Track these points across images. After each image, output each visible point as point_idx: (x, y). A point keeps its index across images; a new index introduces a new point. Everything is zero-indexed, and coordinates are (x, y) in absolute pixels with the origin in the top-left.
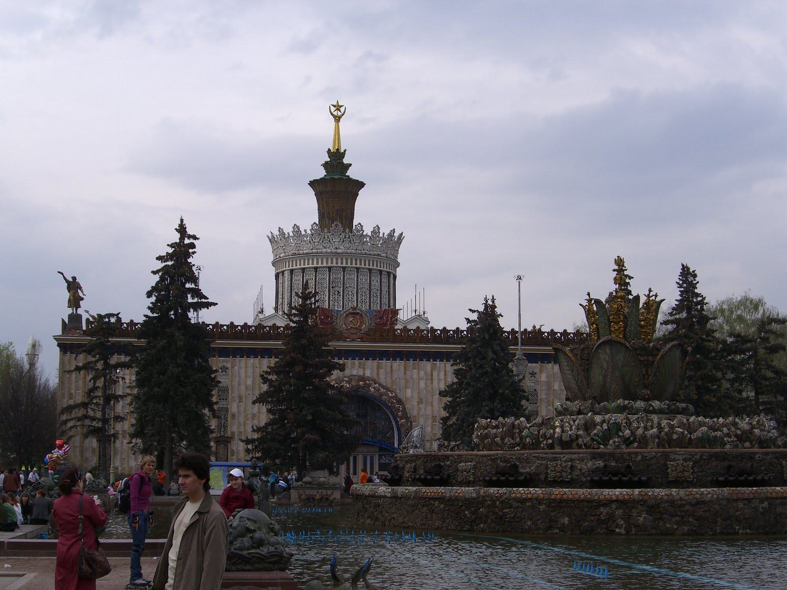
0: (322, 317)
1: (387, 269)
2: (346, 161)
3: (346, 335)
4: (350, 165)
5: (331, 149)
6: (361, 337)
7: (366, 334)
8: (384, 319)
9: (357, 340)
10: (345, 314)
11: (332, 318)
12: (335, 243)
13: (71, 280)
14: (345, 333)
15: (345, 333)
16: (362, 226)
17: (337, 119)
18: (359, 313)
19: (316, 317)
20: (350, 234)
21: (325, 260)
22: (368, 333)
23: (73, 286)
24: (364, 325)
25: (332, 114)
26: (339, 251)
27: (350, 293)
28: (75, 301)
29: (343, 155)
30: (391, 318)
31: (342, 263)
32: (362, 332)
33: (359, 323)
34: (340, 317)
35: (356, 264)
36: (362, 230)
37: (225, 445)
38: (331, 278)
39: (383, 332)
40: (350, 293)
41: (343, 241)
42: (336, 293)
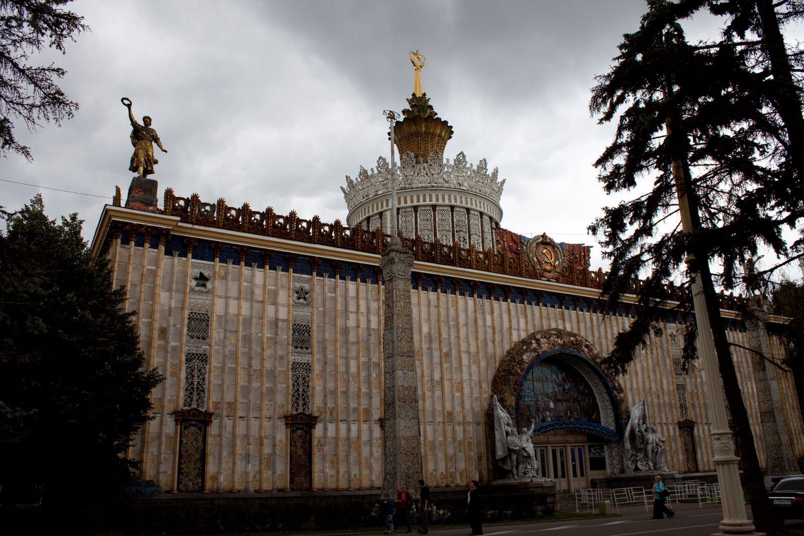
12: (459, 178)
13: (141, 123)
17: (418, 68)
26: (462, 188)
42: (462, 239)
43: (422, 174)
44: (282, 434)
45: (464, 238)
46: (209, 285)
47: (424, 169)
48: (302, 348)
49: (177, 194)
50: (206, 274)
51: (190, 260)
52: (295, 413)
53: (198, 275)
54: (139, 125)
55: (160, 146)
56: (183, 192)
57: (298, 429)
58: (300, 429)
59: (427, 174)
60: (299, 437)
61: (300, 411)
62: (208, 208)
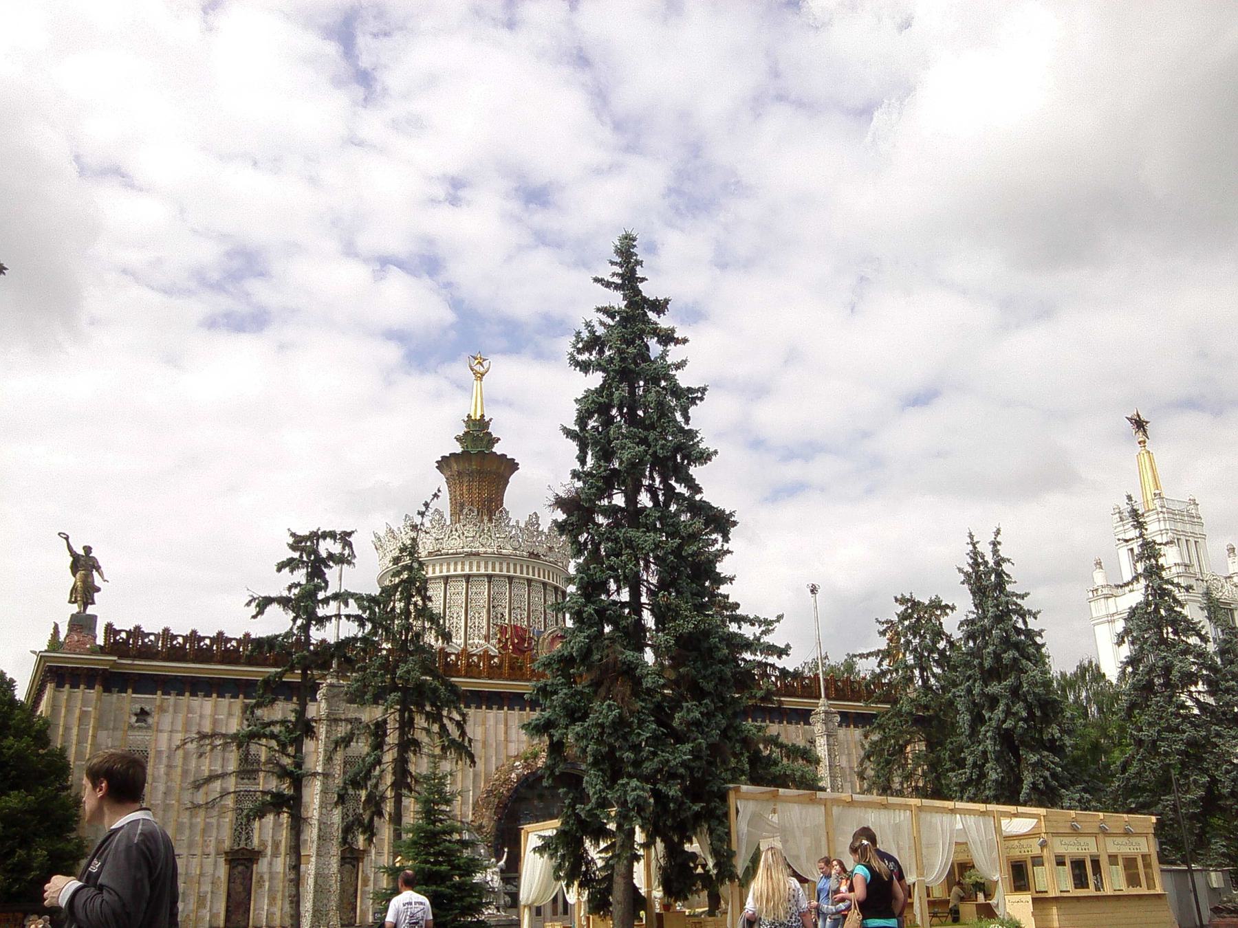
0: (516, 641)
4: (499, 439)
5: (472, 414)
10: (550, 637)
11: (529, 644)
13: (81, 552)
16: (537, 517)
19: (507, 639)
21: (482, 565)
23: (84, 564)
25: (472, 370)
27: (519, 617)
28: (85, 593)
29: (487, 425)
34: (543, 642)
36: (537, 523)
37: (354, 866)
38: (492, 592)
40: (519, 617)
42: (499, 616)
43: (454, 537)
44: (223, 871)
45: (502, 614)
46: (150, 720)
47: (456, 530)
48: (249, 779)
49: (117, 627)
50: (147, 708)
51: (129, 695)
52: (236, 848)
53: (139, 711)
54: (79, 555)
55: (101, 575)
56: (124, 624)
57: (238, 864)
58: (242, 864)
59: (459, 536)
60: (239, 873)
61: (241, 846)
62: (152, 638)
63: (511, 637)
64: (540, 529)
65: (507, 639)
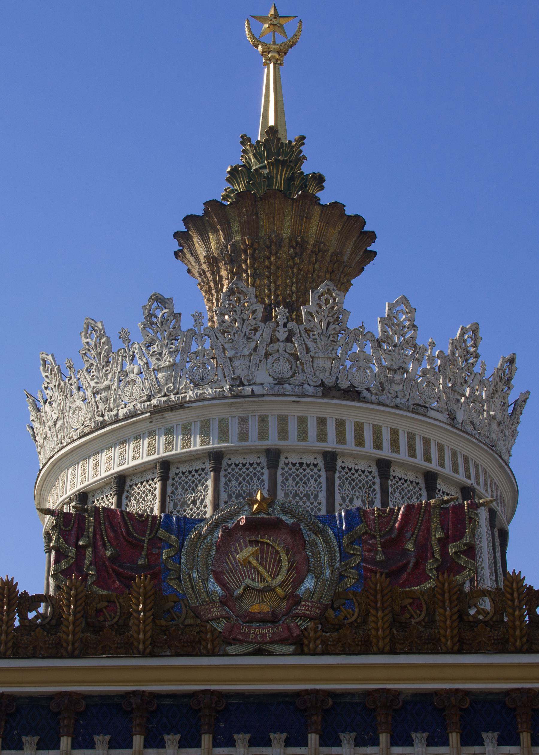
1: (456, 471)
2: (307, 168)
3: (220, 627)
6: (296, 632)
7: (322, 619)
8: (410, 546)
9: (277, 648)
14: (217, 619)
15: (217, 619)
18: (280, 521)
19: (81, 550)
20: (292, 325)
22: (331, 613)
24: (310, 582)
30: (444, 543)
31: (263, 434)
32: (301, 610)
33: (284, 570)
35: (322, 437)
39: (404, 608)
41: (267, 355)
63: (94, 544)
64: (352, 324)
65: (81, 550)
